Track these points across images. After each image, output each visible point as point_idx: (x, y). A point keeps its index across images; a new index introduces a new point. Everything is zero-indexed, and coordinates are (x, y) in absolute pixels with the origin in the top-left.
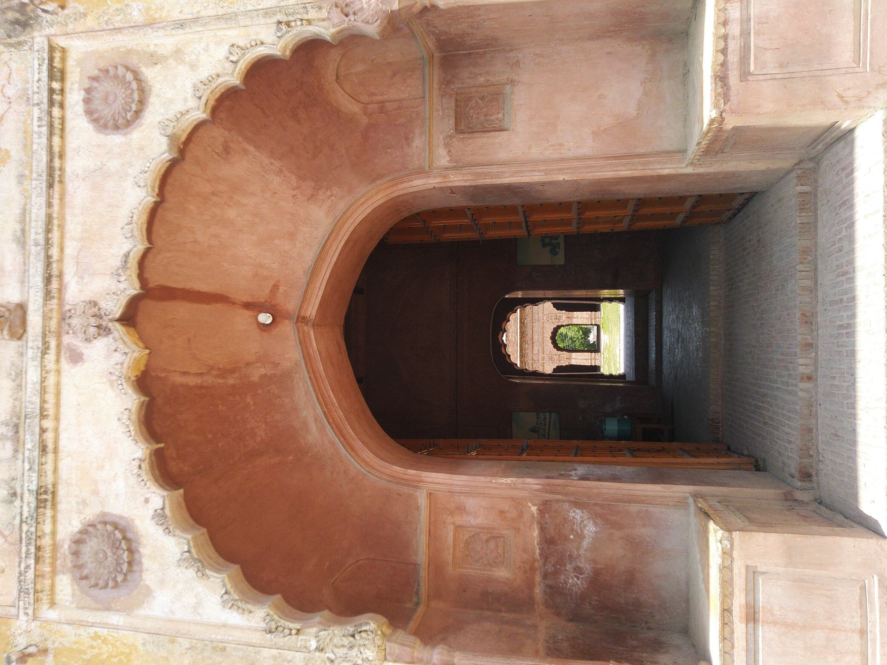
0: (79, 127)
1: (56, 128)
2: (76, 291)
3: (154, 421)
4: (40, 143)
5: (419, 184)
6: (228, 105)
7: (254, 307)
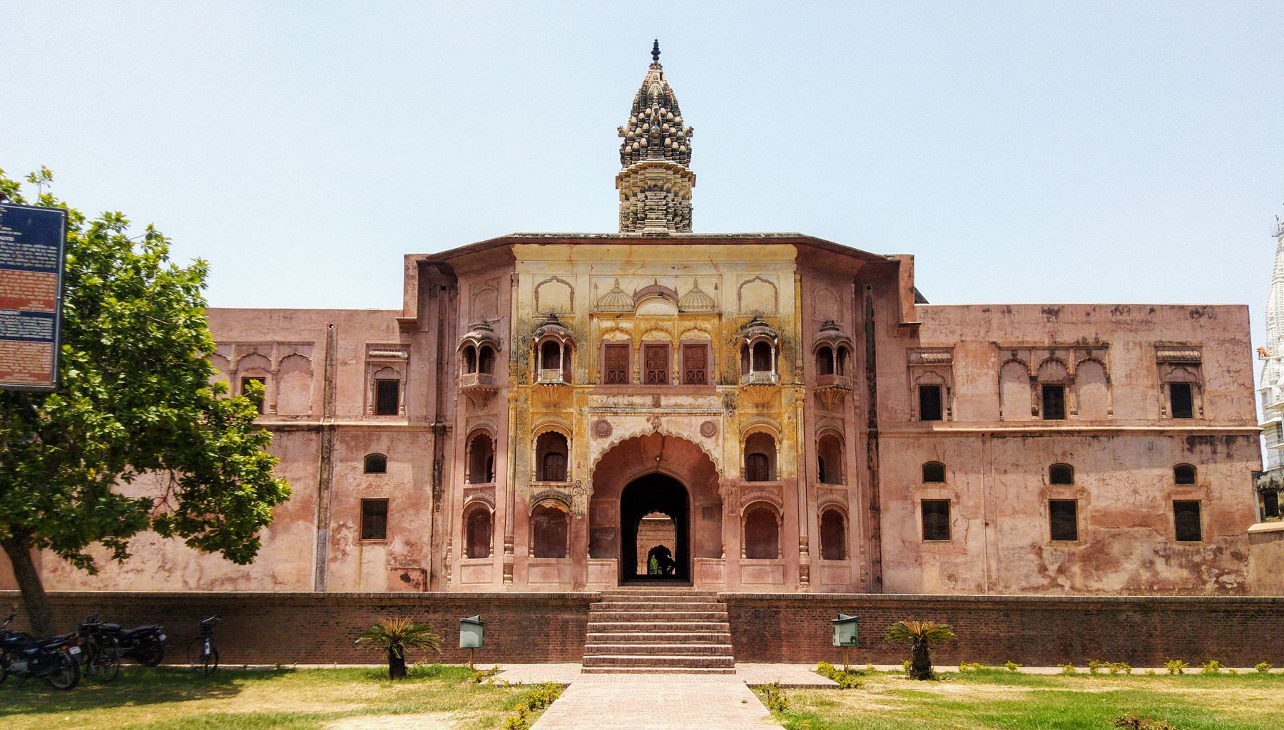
0: (702, 420)
1: (702, 414)
2: (663, 419)
3: (633, 439)
4: (698, 411)
5: (691, 497)
6: (705, 457)
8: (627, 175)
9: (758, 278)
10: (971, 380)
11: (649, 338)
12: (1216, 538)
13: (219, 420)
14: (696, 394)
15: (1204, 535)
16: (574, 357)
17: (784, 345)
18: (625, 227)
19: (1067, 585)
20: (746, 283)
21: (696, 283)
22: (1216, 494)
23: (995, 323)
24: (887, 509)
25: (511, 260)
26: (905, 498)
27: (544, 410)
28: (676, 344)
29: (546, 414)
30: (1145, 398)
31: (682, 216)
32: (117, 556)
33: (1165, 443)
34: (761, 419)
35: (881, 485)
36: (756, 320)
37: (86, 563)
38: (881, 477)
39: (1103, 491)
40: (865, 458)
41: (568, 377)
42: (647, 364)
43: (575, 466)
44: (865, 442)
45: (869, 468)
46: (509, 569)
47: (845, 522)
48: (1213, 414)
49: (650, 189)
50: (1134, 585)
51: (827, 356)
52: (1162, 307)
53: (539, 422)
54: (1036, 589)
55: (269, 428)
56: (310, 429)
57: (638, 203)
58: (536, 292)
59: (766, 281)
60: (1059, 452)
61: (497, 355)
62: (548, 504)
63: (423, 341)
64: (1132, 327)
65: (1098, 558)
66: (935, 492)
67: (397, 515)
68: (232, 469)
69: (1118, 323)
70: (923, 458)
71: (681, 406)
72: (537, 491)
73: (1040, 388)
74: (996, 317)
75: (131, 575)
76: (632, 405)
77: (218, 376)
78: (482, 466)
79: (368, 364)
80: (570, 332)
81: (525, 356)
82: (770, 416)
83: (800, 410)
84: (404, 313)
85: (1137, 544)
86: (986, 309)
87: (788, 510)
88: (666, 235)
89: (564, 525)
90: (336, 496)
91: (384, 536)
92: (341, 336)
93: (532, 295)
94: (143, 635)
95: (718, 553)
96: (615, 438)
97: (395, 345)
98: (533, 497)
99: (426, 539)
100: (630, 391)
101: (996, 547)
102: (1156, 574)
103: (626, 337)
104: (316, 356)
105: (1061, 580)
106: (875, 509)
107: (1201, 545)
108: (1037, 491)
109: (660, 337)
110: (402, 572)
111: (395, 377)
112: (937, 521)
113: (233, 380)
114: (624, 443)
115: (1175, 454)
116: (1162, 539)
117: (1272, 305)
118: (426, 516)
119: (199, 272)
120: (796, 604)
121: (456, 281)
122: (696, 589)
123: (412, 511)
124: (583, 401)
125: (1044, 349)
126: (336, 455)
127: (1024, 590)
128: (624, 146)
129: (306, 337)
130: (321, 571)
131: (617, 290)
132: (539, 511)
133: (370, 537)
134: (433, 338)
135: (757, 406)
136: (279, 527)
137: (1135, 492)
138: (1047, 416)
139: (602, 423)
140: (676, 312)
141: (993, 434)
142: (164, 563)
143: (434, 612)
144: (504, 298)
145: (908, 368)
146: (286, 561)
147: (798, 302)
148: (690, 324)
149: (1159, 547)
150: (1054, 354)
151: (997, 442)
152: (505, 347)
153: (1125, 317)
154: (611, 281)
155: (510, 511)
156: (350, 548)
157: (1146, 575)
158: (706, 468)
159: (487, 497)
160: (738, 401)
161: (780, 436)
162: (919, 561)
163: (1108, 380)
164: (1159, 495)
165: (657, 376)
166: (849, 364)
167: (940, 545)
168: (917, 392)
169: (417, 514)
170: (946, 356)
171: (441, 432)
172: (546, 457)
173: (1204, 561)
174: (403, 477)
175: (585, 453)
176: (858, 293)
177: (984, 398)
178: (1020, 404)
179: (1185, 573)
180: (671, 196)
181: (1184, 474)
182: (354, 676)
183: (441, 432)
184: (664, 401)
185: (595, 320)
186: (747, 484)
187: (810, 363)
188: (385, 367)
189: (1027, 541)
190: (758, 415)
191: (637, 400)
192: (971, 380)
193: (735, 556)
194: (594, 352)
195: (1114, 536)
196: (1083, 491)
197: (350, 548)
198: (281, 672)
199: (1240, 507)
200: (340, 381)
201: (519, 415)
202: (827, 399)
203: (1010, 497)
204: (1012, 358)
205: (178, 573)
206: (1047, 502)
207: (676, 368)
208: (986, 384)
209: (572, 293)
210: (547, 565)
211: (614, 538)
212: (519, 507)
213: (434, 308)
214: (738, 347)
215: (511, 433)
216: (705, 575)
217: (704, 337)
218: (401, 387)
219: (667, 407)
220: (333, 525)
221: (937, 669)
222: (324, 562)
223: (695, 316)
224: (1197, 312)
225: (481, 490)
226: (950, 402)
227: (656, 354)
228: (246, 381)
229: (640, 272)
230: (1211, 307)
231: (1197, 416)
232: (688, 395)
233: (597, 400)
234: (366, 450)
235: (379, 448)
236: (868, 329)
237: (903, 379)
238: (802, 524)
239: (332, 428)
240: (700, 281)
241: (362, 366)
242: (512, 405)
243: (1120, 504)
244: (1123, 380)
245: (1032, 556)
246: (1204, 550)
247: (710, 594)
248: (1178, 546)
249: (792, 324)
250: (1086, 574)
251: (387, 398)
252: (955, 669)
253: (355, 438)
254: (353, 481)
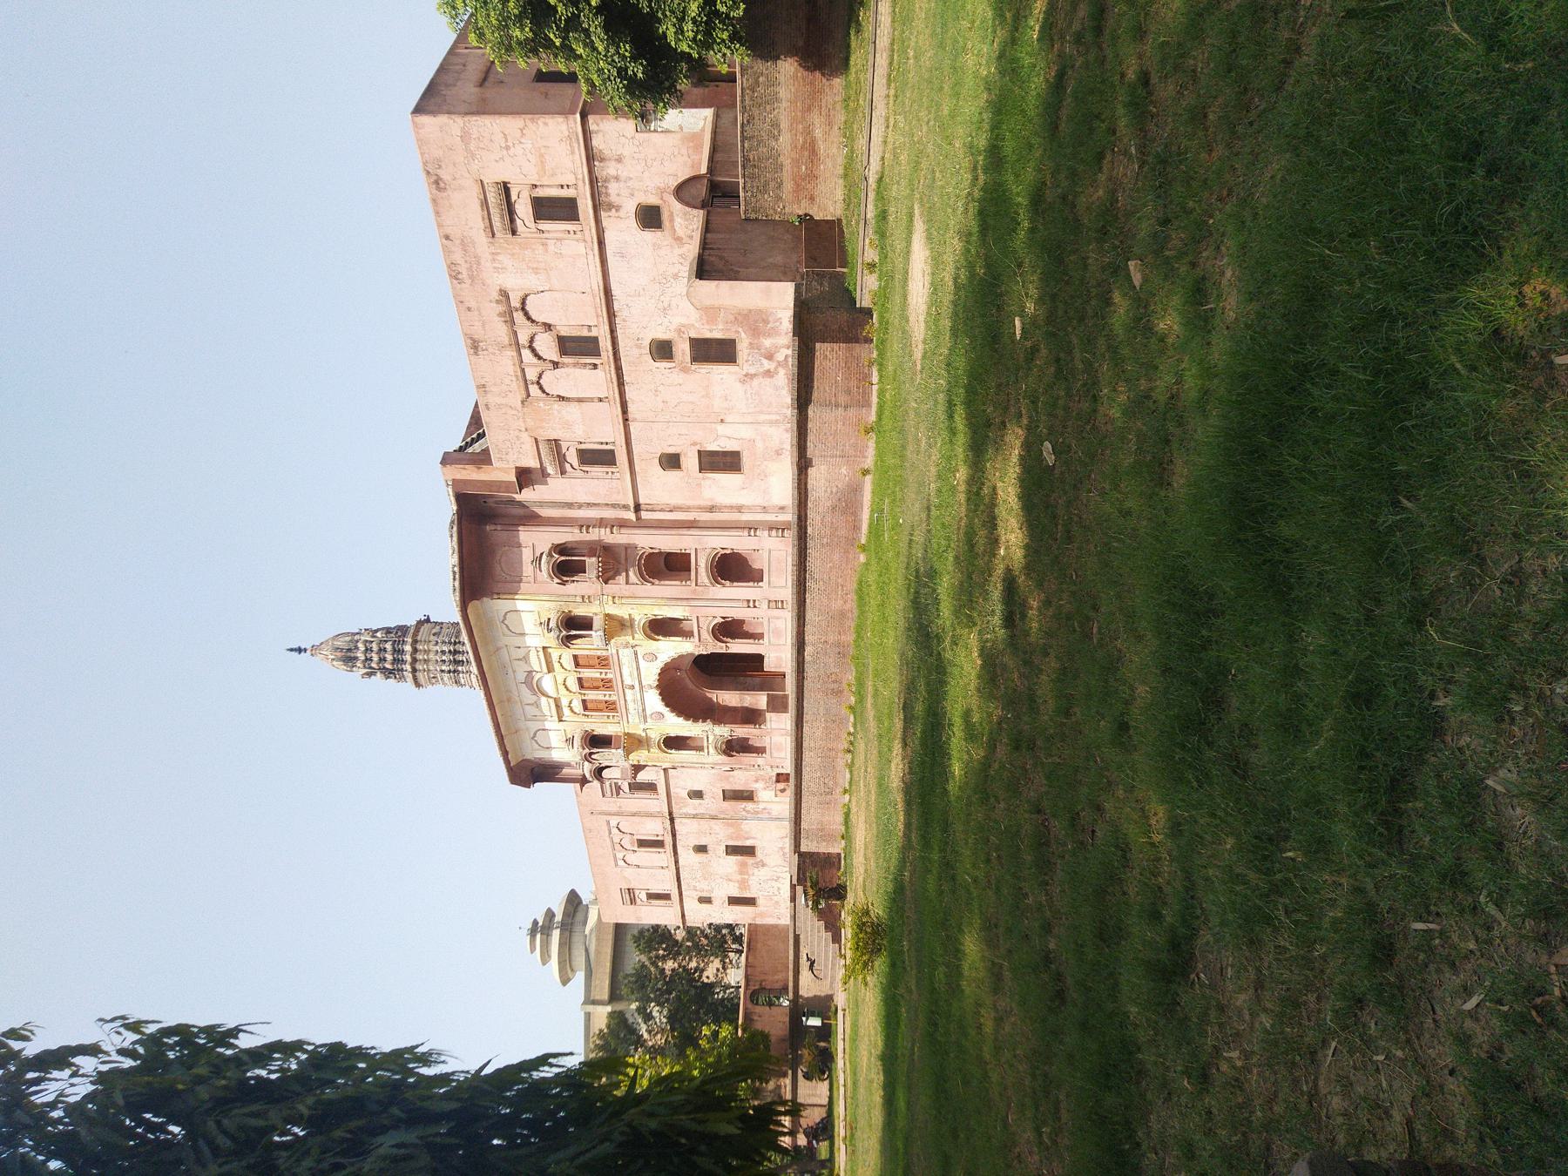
23: (499, 400)
60: (636, 352)
108: (682, 375)
148: (557, 666)
154: (527, 708)
233: (634, 718)
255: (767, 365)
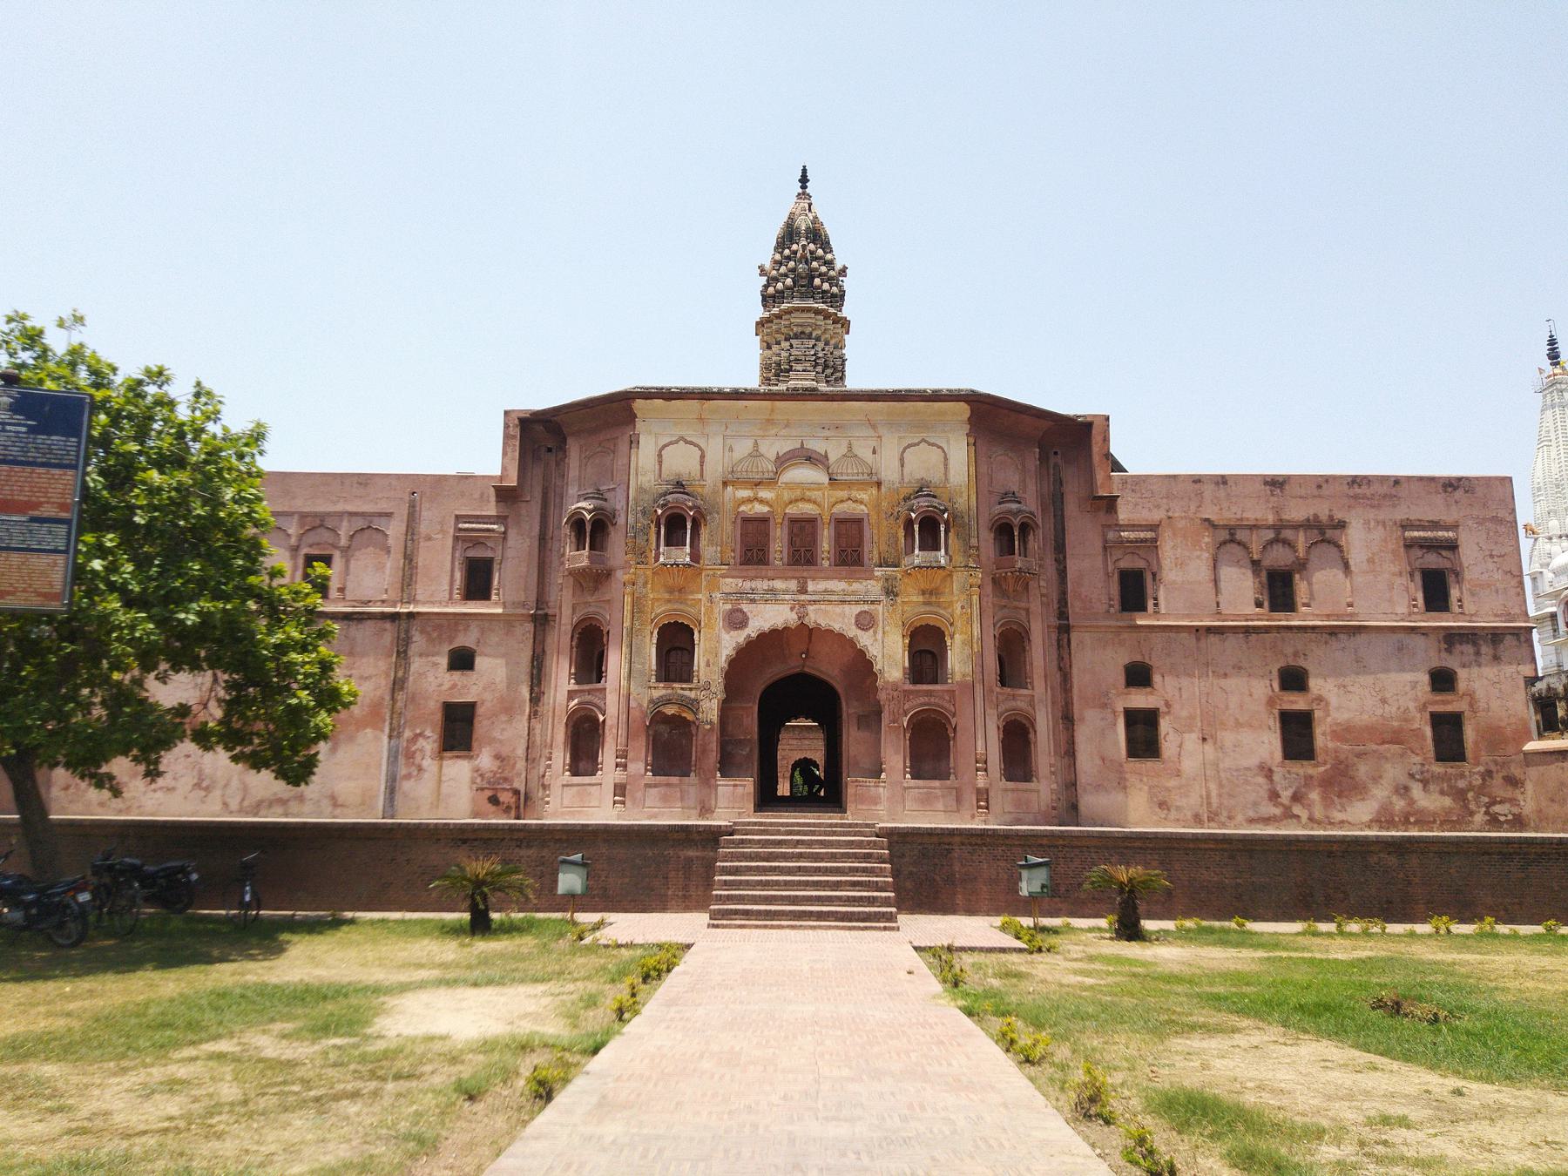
0: (857, 609)
1: (857, 602)
2: (810, 608)
6: (861, 654)
7: (807, 653)
8: (769, 320)
9: (923, 440)
10: (1181, 564)
11: (792, 510)
12: (1484, 758)
13: (273, 608)
14: (850, 578)
15: (1469, 754)
16: (704, 533)
17: (955, 521)
18: (766, 380)
19: (1304, 815)
20: (909, 446)
21: (850, 446)
22: (1482, 705)
24: (1082, 719)
25: (631, 418)
26: (1104, 706)
27: (667, 596)
28: (826, 518)
29: (669, 601)
30: (1391, 587)
31: (833, 368)
32: (148, 774)
33: (1419, 642)
34: (928, 608)
35: (1075, 691)
36: (922, 489)
37: (102, 781)
38: (1075, 681)
39: (1344, 699)
40: (1055, 656)
41: (695, 556)
42: (791, 543)
43: (702, 664)
44: (1054, 636)
45: (1060, 669)
46: (620, 790)
47: (1031, 736)
48: (1474, 607)
49: (796, 337)
50: (1384, 818)
51: (1007, 534)
52: (1409, 478)
53: (660, 609)
54: (1267, 820)
55: (335, 617)
56: (384, 617)
57: (782, 352)
58: (660, 456)
59: (933, 445)
61: (611, 528)
62: (670, 710)
63: (524, 512)
64: (1374, 502)
65: (1341, 783)
66: (1140, 700)
67: (485, 722)
68: (289, 671)
69: (1356, 497)
70: (1124, 657)
71: (833, 592)
72: (656, 694)
73: (1264, 574)
74: (1208, 490)
75: (159, 794)
76: (772, 591)
77: (277, 556)
78: (590, 664)
79: (456, 538)
80: (699, 502)
81: (645, 531)
82: (939, 605)
83: (975, 598)
84: (501, 478)
85: (1388, 766)
86: (1197, 480)
87: (962, 721)
88: (815, 389)
89: (690, 736)
90: (412, 699)
91: (469, 748)
92: (425, 505)
93: (654, 459)
94: (171, 874)
95: (876, 772)
96: (752, 630)
97: (489, 517)
98: (651, 701)
99: (521, 751)
100: (770, 573)
101: (1213, 771)
102: (1412, 802)
103: (765, 509)
104: (395, 530)
105: (1297, 810)
106: (1067, 719)
107: (1466, 767)
108: (1264, 700)
109: (807, 509)
110: (489, 793)
111: (489, 554)
112: (1143, 735)
113: (294, 558)
114: (762, 636)
115: (1431, 655)
116: (1418, 759)
117: (1539, 473)
118: (521, 724)
119: (257, 436)
120: (973, 840)
121: (564, 441)
122: (849, 819)
123: (504, 718)
124: (714, 586)
125: (1269, 527)
126: (414, 649)
127: (1251, 821)
128: (766, 287)
129: (383, 506)
130: (391, 790)
131: (756, 454)
132: (658, 718)
133: (452, 749)
134: (535, 509)
135: (924, 593)
136: (342, 737)
137: (1384, 701)
138: (1273, 608)
139: (737, 614)
140: (825, 479)
141: (1209, 630)
142: (201, 779)
143: (529, 847)
144: (621, 461)
145: (1105, 548)
146: (350, 782)
147: (972, 469)
148: (844, 494)
149: (1415, 769)
150: (1280, 533)
151: (1213, 639)
152: (621, 520)
153: (1364, 490)
154: (749, 443)
155: (623, 717)
156: (428, 763)
157: (1399, 804)
158: (862, 666)
159: (596, 700)
160: (900, 587)
161: (951, 629)
162: (1122, 785)
163: (1346, 566)
164: (1412, 705)
165: (802, 556)
166: (1034, 544)
167: (1148, 765)
168: (1116, 577)
169: (510, 721)
170: (1149, 535)
171: (542, 621)
172: (669, 652)
173: (1471, 788)
174: (494, 676)
175: (715, 649)
176: (1043, 458)
177: (1198, 587)
178: (1240, 595)
179: (1447, 802)
180: (821, 345)
181: (1442, 680)
182: (426, 929)
183: (542, 621)
184: (811, 586)
185: (730, 488)
186: (912, 687)
187: (987, 542)
188: (477, 543)
189: (1253, 761)
190: (925, 603)
191: (779, 584)
192: (1181, 564)
193: (897, 776)
194: (728, 527)
195: (1359, 755)
196: (1320, 699)
197: (428, 763)
198: (337, 923)
199: (1513, 720)
200: (421, 560)
201: (637, 604)
202: (1007, 586)
203: (1232, 706)
204: (1229, 538)
205: (217, 793)
206: (1276, 712)
207: (826, 546)
208: (1199, 568)
209: (703, 457)
210: (668, 785)
211: (750, 752)
212: (635, 714)
213: (537, 472)
214: (901, 522)
215: (627, 624)
216: (862, 799)
217: (860, 510)
218: (496, 567)
219: (815, 593)
220: (408, 734)
221: (1149, 925)
222: (394, 780)
223: (849, 485)
224: (1451, 485)
225: (589, 692)
226: (1156, 591)
227: (802, 529)
228: (309, 560)
229: (784, 432)
230: (1467, 478)
231: (1456, 609)
232: (840, 579)
233: (730, 584)
234: (451, 643)
235: (466, 640)
236: (1055, 503)
237: (1099, 562)
238: (980, 739)
239: (411, 615)
240: (855, 443)
241: (450, 542)
242: (628, 590)
243: (1365, 717)
244: (1365, 566)
245: (1261, 780)
246: (1471, 773)
247: (867, 826)
248: (1438, 768)
249: (965, 495)
250: (1327, 802)
251: (477, 581)
252: (1169, 925)
253: (438, 627)
254: (434, 680)
255: (1286, 795)
